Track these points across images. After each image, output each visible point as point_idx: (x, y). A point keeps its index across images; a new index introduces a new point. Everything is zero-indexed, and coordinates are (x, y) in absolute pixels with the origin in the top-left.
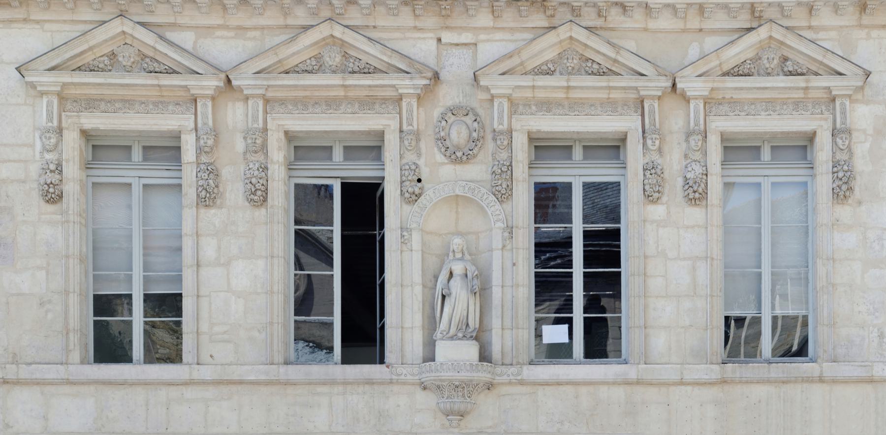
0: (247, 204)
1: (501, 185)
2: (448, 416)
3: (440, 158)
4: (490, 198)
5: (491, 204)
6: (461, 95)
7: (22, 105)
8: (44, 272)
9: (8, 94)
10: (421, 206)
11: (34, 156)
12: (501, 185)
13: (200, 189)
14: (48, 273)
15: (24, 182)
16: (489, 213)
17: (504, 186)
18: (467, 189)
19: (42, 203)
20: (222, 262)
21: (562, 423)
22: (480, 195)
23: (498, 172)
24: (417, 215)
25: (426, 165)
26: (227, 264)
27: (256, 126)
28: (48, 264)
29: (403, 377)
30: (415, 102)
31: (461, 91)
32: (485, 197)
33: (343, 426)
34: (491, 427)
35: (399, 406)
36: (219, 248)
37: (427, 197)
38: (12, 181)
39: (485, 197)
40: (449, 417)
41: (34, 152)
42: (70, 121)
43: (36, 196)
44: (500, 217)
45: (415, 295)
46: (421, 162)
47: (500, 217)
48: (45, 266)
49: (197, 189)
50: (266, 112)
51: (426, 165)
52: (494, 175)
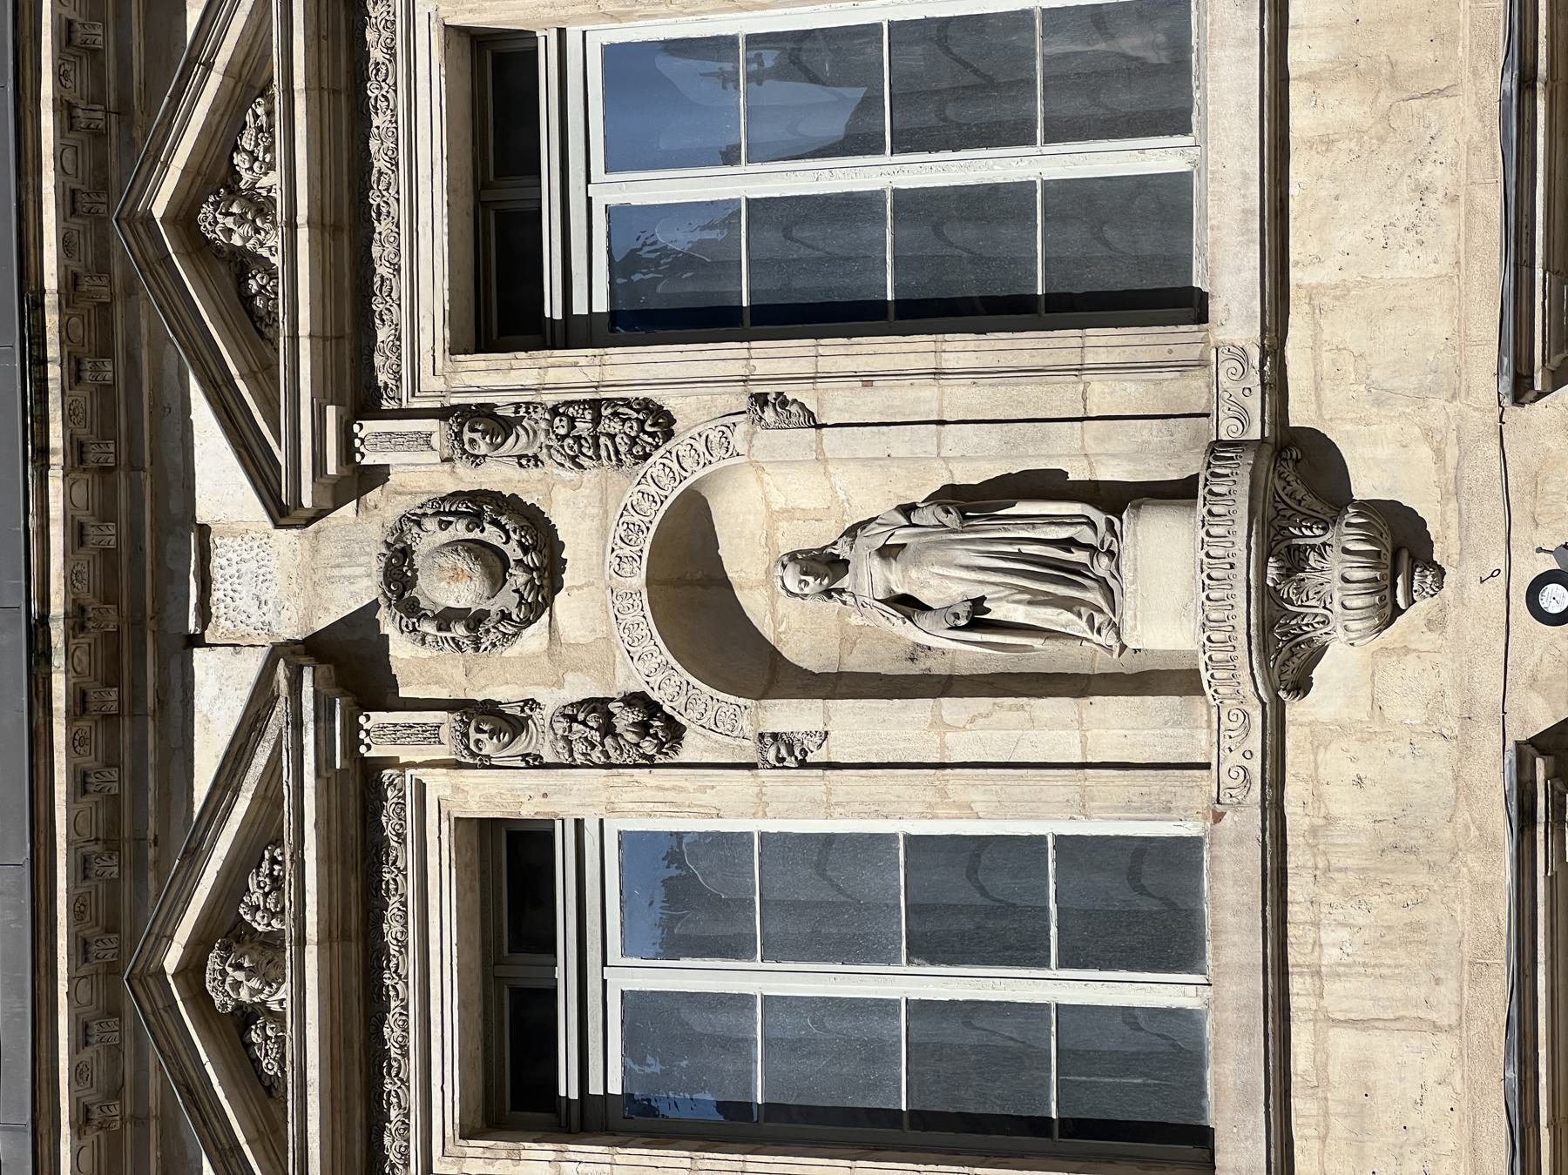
1: (612, 437)
2: (1396, 605)
3: (534, 638)
4: (657, 471)
5: (675, 466)
6: (346, 571)
10: (683, 699)
12: (612, 437)
16: (701, 473)
17: (615, 426)
18: (627, 551)
21: (1423, 191)
22: (646, 505)
23: (571, 448)
24: (710, 714)
25: (559, 684)
29: (1255, 766)
30: (368, 718)
31: (336, 572)
32: (653, 489)
33: (1438, 981)
34: (1439, 454)
35: (1359, 782)
37: (656, 680)
39: (653, 489)
40: (1402, 605)
44: (715, 437)
45: (972, 721)
46: (552, 699)
47: (715, 437)
51: (559, 684)
52: (582, 460)
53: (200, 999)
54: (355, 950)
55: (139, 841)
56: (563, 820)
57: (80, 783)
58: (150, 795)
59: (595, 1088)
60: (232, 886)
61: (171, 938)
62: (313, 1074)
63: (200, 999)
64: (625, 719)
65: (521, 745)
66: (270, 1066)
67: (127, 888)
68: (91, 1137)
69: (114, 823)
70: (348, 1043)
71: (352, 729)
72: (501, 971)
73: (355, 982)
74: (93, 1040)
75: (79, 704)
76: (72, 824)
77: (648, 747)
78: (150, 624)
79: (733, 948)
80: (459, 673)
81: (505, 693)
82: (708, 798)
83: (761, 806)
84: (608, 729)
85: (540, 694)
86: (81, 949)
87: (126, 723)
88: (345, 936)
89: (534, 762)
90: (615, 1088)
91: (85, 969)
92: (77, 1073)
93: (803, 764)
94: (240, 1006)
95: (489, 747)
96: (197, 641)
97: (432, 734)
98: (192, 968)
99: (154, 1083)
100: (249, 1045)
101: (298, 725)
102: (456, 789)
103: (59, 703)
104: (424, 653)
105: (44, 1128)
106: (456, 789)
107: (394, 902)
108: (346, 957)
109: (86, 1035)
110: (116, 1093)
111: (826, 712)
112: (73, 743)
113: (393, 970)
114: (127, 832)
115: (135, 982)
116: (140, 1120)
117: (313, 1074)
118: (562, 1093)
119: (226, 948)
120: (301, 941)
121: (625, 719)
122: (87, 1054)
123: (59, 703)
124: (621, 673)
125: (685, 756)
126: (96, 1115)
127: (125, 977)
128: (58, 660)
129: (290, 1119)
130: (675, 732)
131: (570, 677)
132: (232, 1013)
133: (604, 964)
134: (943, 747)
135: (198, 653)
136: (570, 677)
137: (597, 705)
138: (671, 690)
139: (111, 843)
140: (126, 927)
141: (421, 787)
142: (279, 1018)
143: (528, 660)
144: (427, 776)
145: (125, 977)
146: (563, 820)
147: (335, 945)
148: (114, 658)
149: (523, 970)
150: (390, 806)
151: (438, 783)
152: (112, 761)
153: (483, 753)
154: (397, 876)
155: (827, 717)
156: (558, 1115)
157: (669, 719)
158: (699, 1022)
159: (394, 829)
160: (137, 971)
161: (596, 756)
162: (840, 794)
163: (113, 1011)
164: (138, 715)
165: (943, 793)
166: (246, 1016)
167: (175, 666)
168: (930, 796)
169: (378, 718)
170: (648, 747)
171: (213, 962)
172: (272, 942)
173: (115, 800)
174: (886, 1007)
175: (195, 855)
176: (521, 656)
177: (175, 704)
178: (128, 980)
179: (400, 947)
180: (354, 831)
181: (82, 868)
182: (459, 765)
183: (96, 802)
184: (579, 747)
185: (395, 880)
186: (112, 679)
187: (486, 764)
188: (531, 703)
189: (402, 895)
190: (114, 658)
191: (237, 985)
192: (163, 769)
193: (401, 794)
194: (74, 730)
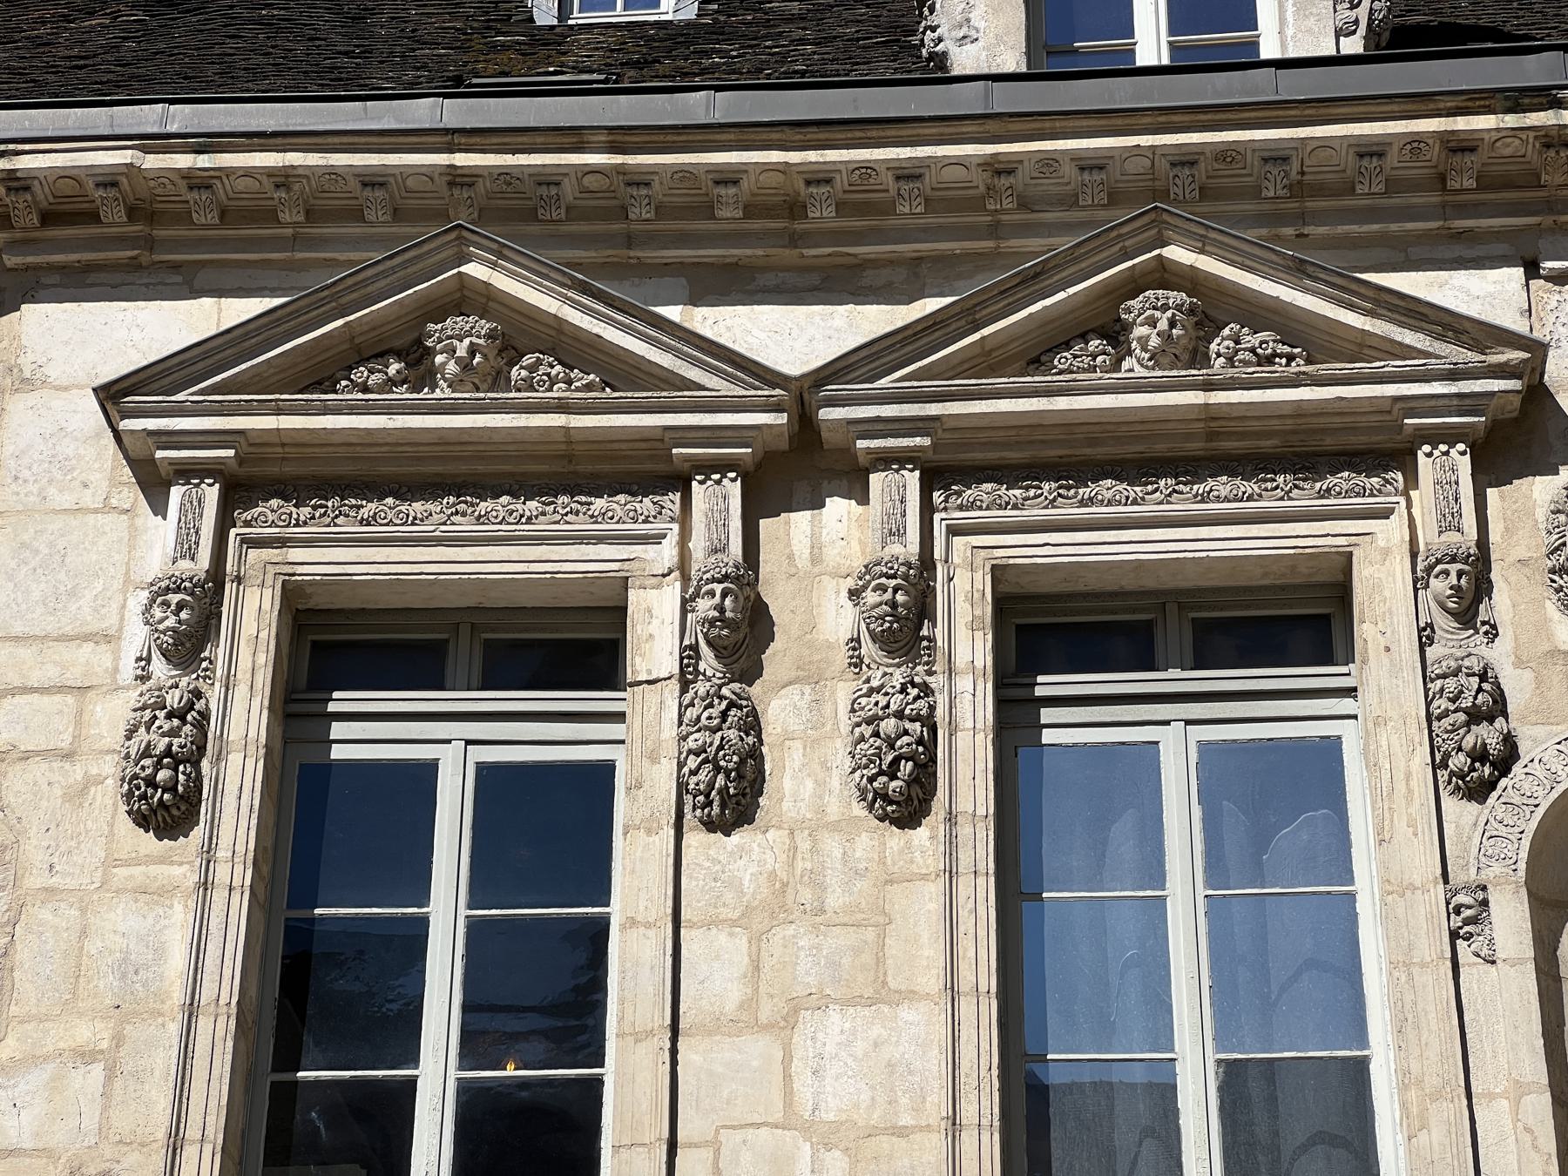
0: (859, 810)
7: (96, 511)
8: (98, 1070)
9: (50, 481)
10: (1517, 800)
11: (116, 670)
13: (693, 763)
14: (110, 1075)
15: (68, 756)
19: (125, 824)
20: (763, 1017)
24: (1503, 831)
25: (1519, 663)
26: (788, 1022)
27: (896, 549)
28: (118, 1040)
30: (1463, 453)
36: (757, 967)
37: (1536, 768)
38: (26, 756)
41: (117, 659)
42: (253, 554)
43: (108, 803)
45: (1528, 1130)
46: (1500, 655)
48: (104, 1045)
49: (681, 765)
50: (927, 509)
51: (1519, 663)
53: (1133, 286)
54: (1196, 447)
55: (1302, 218)
56: (1349, 674)
57: (1371, 150)
58: (1355, 228)
59: (1047, 715)
60: (1259, 313)
61: (1202, 251)
62: (1062, 403)
63: (1133, 286)
64: (1488, 735)
65: (1443, 622)
66: (1062, 360)
67: (1249, 207)
68: (980, 179)
69: (1320, 190)
70: (1093, 442)
71: (1449, 436)
72: (1172, 609)
73: (1161, 448)
74: (1086, 176)
75: (1460, 145)
76: (1325, 143)
77: (1459, 761)
78: (1547, 220)
79: (1216, 868)
80: (1521, 552)
81: (1502, 604)
82: (1401, 826)
83: (1395, 888)
84: (1475, 716)
85: (1504, 643)
86: (1186, 159)
87: (1434, 198)
88: (1212, 435)
89: (1426, 635)
90: (1048, 736)
91: (1163, 165)
92: (1049, 160)
93: (1454, 935)
94: (1127, 328)
95: (1439, 586)
96: (1532, 270)
97: (1450, 522)
98: (1165, 276)
99: (1034, 243)
100: (1084, 337)
101: (1453, 375)
102: (1386, 552)
103: (1462, 123)
104: (1541, 514)
105: (992, 126)
106: (1386, 552)
107: (1251, 487)
108: (1189, 437)
109: (1091, 169)
110: (1024, 204)
111: (1519, 962)
112: (1416, 140)
113: (1176, 488)
114: (1310, 204)
115: (1153, 215)
116: (995, 230)
117: (1062, 403)
118: (1040, 679)
119: (1192, 311)
120: (1208, 386)
121: (1488, 735)
122: (1069, 170)
123: (1462, 123)
124: (1540, 731)
125: (1450, 804)
126: (1004, 181)
127: (1159, 205)
128: (1511, 120)
129: (1012, 380)
130: (1478, 792)
131: (1528, 675)
132: (1119, 319)
133: (1188, 722)
134: (1491, 1096)
135: (1518, 273)
136: (1528, 675)
137: (1499, 707)
138: (1526, 787)
139: (1299, 189)
140: (1205, 207)
141: (1385, 514)
142: (1116, 366)
143: (1543, 627)
144: (1397, 524)
145: (1159, 205)
146: (1349, 674)
147: (1202, 425)
148: (1507, 184)
149: (1175, 634)
150: (1361, 480)
151: (1391, 531)
152: (1393, 186)
153: (1432, 580)
154: (1282, 490)
155: (1519, 962)
156: (1015, 675)
157: (1492, 785)
158: (1123, 831)
159: (1335, 485)
160: (1165, 217)
161: (1442, 704)
162: (1424, 978)
163: (1115, 198)
164: (1444, 211)
165: (1436, 1096)
166: (1116, 335)
167: (1501, 248)
168: (1432, 1081)
169: (1464, 465)
170: (1459, 761)
171: (1176, 297)
172: (1198, 358)
173: (1351, 190)
174: (1163, 1035)
175: (1298, 272)
176: (1546, 620)
177: (1459, 250)
178: (1156, 207)
179: (1202, 495)
180: (1330, 442)
181: (1276, 156)
182: (1414, 555)
183: (1344, 171)
184: (1451, 684)
185: (1277, 488)
186: (1485, 183)
187: (1419, 583)
188: (1493, 633)
189: (1260, 495)
190: (1507, 184)
191: (1152, 323)
192: (1384, 240)
193: (1375, 492)
194: (1430, 142)
